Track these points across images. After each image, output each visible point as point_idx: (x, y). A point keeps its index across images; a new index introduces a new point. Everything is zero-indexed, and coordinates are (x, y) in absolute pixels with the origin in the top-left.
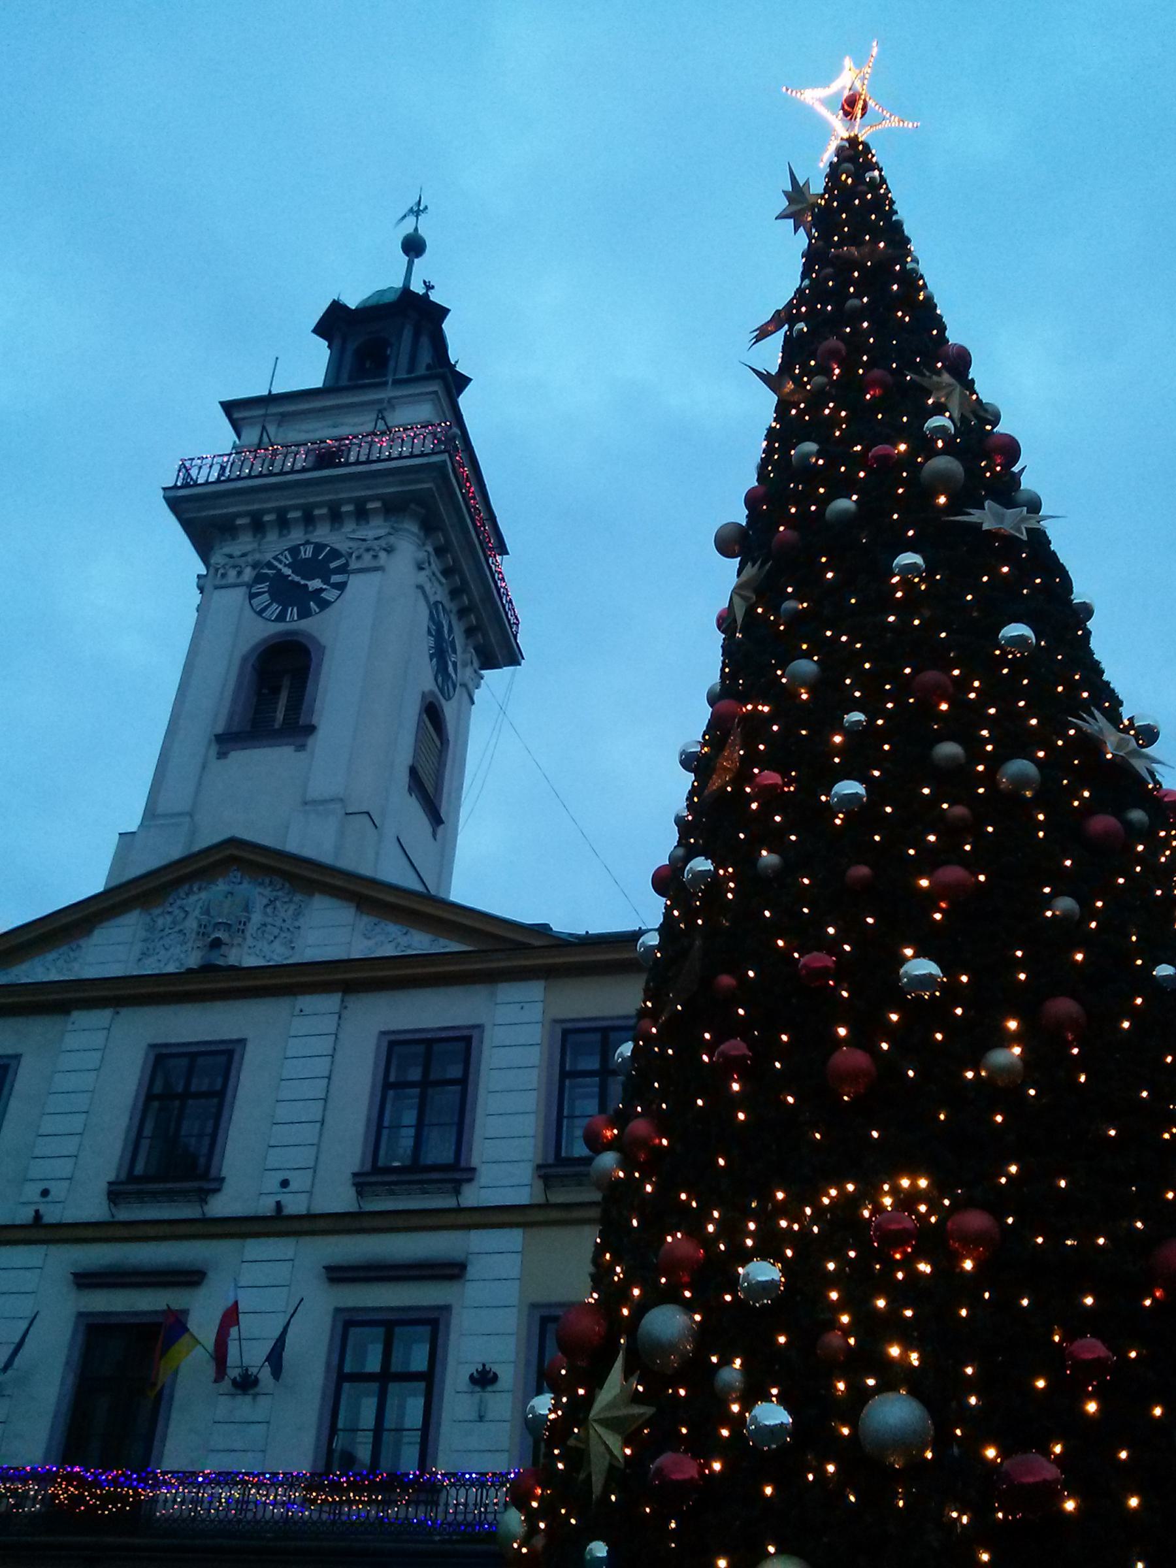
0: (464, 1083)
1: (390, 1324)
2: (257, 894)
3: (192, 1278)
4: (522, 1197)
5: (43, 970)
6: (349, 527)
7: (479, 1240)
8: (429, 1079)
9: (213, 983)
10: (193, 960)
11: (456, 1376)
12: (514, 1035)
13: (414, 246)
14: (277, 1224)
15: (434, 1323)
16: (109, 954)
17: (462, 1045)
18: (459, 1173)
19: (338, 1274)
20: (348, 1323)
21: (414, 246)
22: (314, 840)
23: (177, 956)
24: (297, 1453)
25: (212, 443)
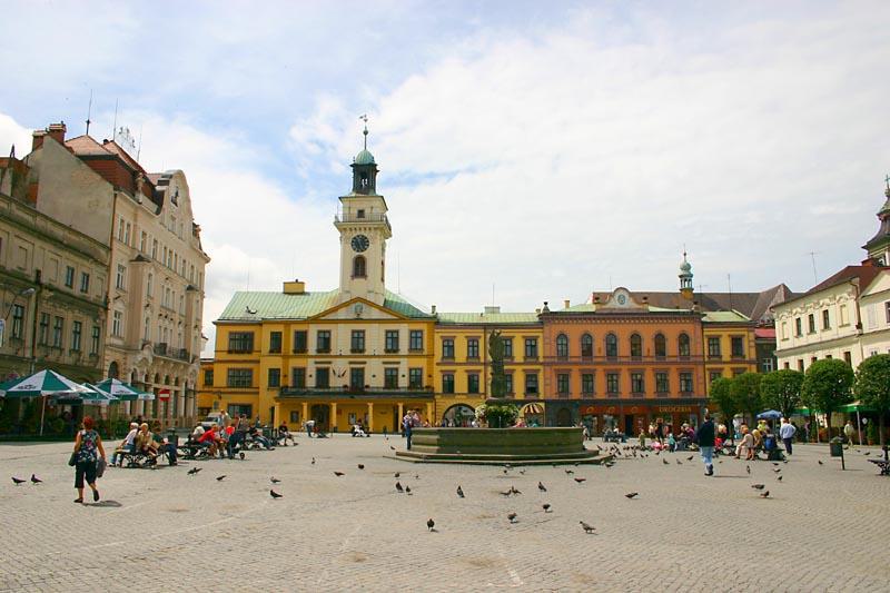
0: (397, 338)
1: (392, 369)
2: (364, 306)
3: (365, 363)
4: (407, 353)
5: (331, 317)
6: (368, 231)
7: (401, 360)
8: (392, 338)
9: (358, 320)
10: (355, 317)
11: (400, 376)
12: (404, 331)
13: (366, 133)
14: (374, 356)
15: (397, 369)
16: (341, 314)
17: (397, 332)
18: (396, 350)
19: (384, 363)
20: (386, 369)
21: (366, 133)
22: (371, 298)
23: (353, 316)
24: (383, 385)
25: (338, 210)
